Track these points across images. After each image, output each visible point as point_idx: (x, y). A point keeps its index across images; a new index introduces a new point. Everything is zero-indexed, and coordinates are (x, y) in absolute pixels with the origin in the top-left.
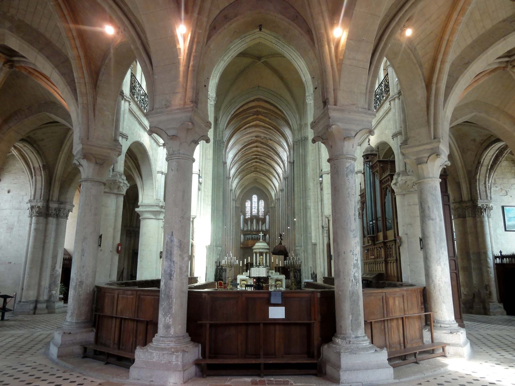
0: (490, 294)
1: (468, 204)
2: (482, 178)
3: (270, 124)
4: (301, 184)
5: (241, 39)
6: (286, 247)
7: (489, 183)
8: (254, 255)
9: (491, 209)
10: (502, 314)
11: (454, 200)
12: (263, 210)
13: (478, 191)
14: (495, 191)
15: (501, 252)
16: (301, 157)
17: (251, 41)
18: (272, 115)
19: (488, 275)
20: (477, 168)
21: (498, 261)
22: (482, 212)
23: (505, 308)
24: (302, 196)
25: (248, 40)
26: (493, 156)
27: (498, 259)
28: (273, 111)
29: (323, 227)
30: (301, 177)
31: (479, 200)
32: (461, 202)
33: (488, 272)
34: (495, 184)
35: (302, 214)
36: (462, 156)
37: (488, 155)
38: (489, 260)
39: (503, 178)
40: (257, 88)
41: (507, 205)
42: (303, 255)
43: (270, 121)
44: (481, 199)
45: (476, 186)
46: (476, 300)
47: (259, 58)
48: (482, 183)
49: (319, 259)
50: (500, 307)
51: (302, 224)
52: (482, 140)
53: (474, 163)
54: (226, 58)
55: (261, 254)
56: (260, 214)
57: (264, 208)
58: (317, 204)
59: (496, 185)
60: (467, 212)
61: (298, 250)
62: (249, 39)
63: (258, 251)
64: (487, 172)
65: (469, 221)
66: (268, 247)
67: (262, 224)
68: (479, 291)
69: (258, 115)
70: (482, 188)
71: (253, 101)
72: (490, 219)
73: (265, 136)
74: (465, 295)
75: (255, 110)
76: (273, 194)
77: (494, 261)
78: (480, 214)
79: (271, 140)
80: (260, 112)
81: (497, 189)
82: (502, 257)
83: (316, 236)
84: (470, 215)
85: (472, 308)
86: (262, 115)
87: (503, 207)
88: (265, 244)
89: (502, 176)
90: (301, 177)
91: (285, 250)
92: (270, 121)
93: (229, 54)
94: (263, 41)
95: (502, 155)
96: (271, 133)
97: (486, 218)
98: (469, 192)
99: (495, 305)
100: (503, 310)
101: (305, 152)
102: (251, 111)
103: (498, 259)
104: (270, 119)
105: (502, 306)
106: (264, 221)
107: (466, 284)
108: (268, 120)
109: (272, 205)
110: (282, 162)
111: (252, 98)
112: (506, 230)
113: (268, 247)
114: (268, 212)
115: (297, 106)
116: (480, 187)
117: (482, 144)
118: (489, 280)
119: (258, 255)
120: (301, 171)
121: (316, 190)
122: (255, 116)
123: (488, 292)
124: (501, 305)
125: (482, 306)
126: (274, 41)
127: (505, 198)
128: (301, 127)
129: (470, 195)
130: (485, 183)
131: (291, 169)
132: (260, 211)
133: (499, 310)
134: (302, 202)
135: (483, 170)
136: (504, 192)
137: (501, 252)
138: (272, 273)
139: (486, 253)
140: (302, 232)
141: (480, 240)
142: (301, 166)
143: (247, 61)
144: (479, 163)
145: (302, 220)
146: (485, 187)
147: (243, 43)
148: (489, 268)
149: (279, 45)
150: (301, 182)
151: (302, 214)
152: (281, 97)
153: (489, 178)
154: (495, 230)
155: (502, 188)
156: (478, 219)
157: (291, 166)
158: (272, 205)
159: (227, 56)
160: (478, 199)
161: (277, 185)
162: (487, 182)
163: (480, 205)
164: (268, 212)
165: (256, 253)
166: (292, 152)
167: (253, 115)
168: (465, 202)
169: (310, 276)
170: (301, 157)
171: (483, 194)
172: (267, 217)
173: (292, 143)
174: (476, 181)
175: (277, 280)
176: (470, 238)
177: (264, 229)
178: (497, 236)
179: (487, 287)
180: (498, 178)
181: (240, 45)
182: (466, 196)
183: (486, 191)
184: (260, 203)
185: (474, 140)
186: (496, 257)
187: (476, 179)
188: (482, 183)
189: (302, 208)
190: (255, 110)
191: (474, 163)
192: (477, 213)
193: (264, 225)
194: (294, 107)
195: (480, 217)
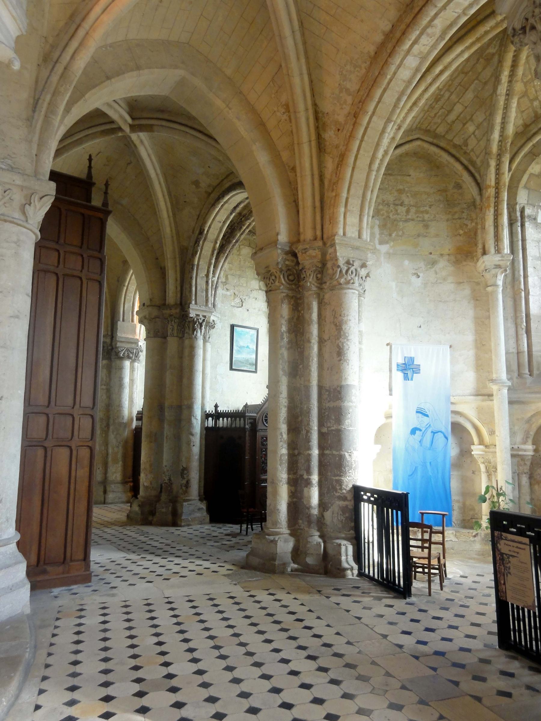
0: (187, 485)
1: (173, 311)
2: (203, 265)
7: (214, 276)
9: (211, 326)
10: (201, 523)
11: (151, 300)
13: (194, 289)
14: (225, 296)
15: (216, 406)
19: (190, 450)
20: (197, 242)
21: (210, 422)
22: (194, 329)
23: (209, 510)
26: (224, 222)
27: (210, 419)
31: (193, 306)
32: (163, 305)
33: (189, 443)
34: (225, 283)
36: (174, 214)
37: (218, 218)
38: (194, 421)
39: (240, 276)
41: (240, 324)
44: (196, 303)
45: (191, 278)
46: (164, 497)
48: (202, 274)
50: (199, 509)
52: (209, 186)
53: (193, 232)
59: (227, 286)
60: (170, 327)
64: (213, 254)
65: (172, 342)
68: (170, 480)
70: (201, 283)
72: (208, 345)
74: (146, 488)
77: (203, 422)
78: (191, 332)
81: (228, 293)
82: (217, 415)
84: (175, 332)
85: (153, 513)
87: (232, 327)
89: (238, 273)
95: (241, 228)
97: (200, 342)
98: (179, 288)
99: (194, 506)
100: (205, 513)
103: (210, 419)
105: (205, 508)
107: (151, 466)
112: (231, 369)
116: (198, 281)
117: (209, 194)
118: (189, 459)
123: (184, 482)
124: (203, 506)
125: (170, 508)
127: (238, 311)
129: (179, 295)
130: (207, 276)
133: (198, 515)
135: (207, 248)
136: (238, 300)
137: (216, 406)
139: (190, 407)
141: (185, 381)
144: (201, 232)
146: (207, 282)
148: (193, 435)
153: (215, 267)
154: (214, 367)
155: (237, 293)
156: (187, 342)
160: (190, 303)
162: (211, 275)
163: (192, 314)
168: (170, 307)
171: (201, 295)
174: (193, 269)
176: (169, 378)
178: (216, 378)
179: (184, 472)
180: (232, 275)
182: (172, 297)
183: (207, 290)
185: (196, 183)
186: (207, 416)
187: (193, 265)
188: (202, 274)
191: (193, 232)
192: (187, 330)
195: (191, 338)
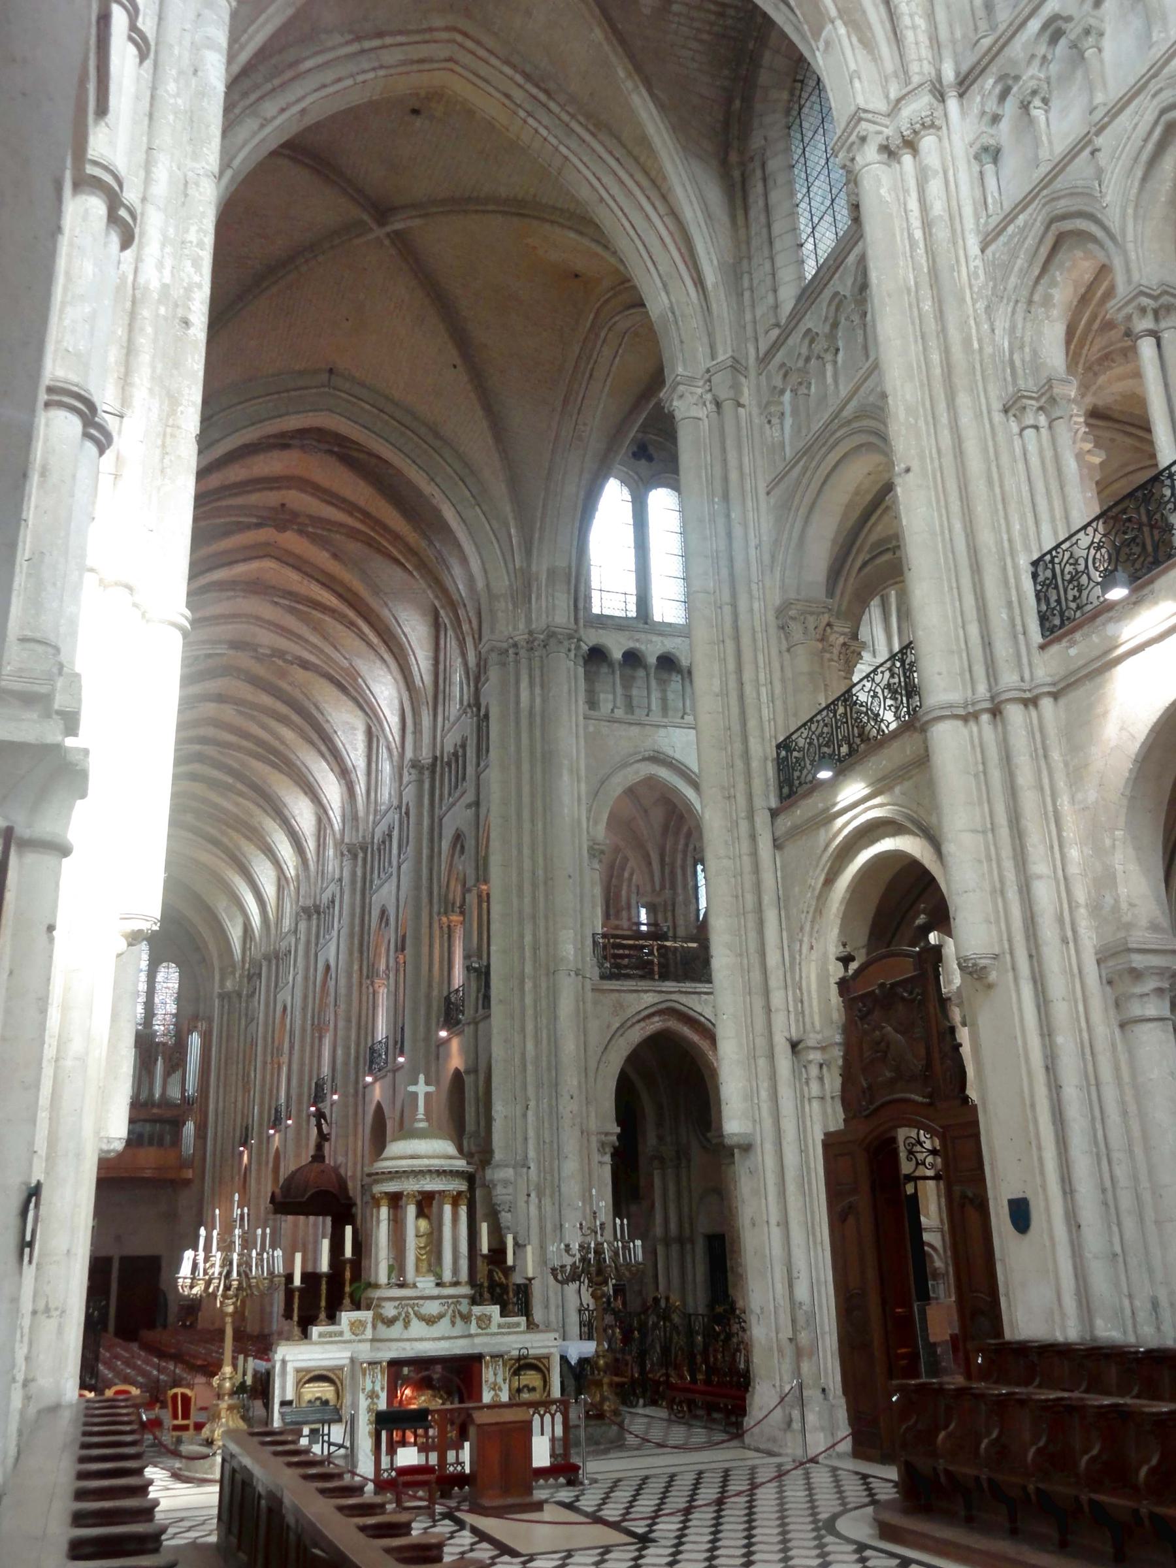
3: (328, 582)
4: (526, 851)
5: (358, 39)
6: (348, 1172)
8: (384, 1211)
12: (172, 1008)
16: (524, 722)
17: (404, 63)
18: (353, 534)
24: (527, 909)
25: (392, 57)
28: (366, 516)
29: (794, 1046)
30: (526, 815)
35: (529, 1000)
40: (325, 376)
42: (533, 1210)
43: (334, 567)
47: (382, 212)
49: (776, 1232)
51: (530, 1046)
54: (270, 108)
55: (426, 1203)
56: (159, 1027)
57: (179, 1000)
58: (751, 920)
61: (506, 1183)
62: (396, 55)
63: (411, 1186)
66: (461, 1164)
67: (167, 1074)
69: (282, 527)
71: (282, 442)
73: (283, 643)
75: (272, 498)
76: (235, 934)
79: (305, 665)
80: (295, 514)
83: (751, 1096)
86: (301, 532)
88: (448, 1147)
90: (526, 815)
91: (342, 1184)
92: (334, 567)
93: (290, 96)
94: (459, 87)
96: (317, 628)
101: (544, 700)
102: (254, 498)
104: (335, 556)
106: (175, 1056)
108: (321, 558)
109: (229, 985)
110: (345, 774)
111: (294, 422)
113: (461, 1164)
114: (196, 1017)
115: (514, 484)
119: (411, 1210)
120: (526, 789)
121: (745, 847)
122: (266, 534)
126: (518, 95)
128: (528, 585)
131: (420, 796)
132: (160, 1011)
134: (528, 939)
138: (484, 1321)
140: (531, 1091)
142: (526, 767)
143: (322, 207)
145: (530, 1027)
147: (366, 65)
149: (546, 120)
150: (526, 839)
151: (529, 1000)
152: (437, 435)
157: (420, 782)
158: (229, 985)
159: (281, 102)
161: (269, 890)
164: (196, 1017)
165: (395, 1200)
166: (426, 721)
167: (258, 526)
169: (573, 1319)
170: (524, 722)
172: (195, 1041)
173: (428, 679)
175: (523, 1364)
177: (175, 1093)
181: (352, 67)
184: (160, 977)
189: (528, 969)
190: (272, 498)
193: (177, 1076)
194: (499, 489)
